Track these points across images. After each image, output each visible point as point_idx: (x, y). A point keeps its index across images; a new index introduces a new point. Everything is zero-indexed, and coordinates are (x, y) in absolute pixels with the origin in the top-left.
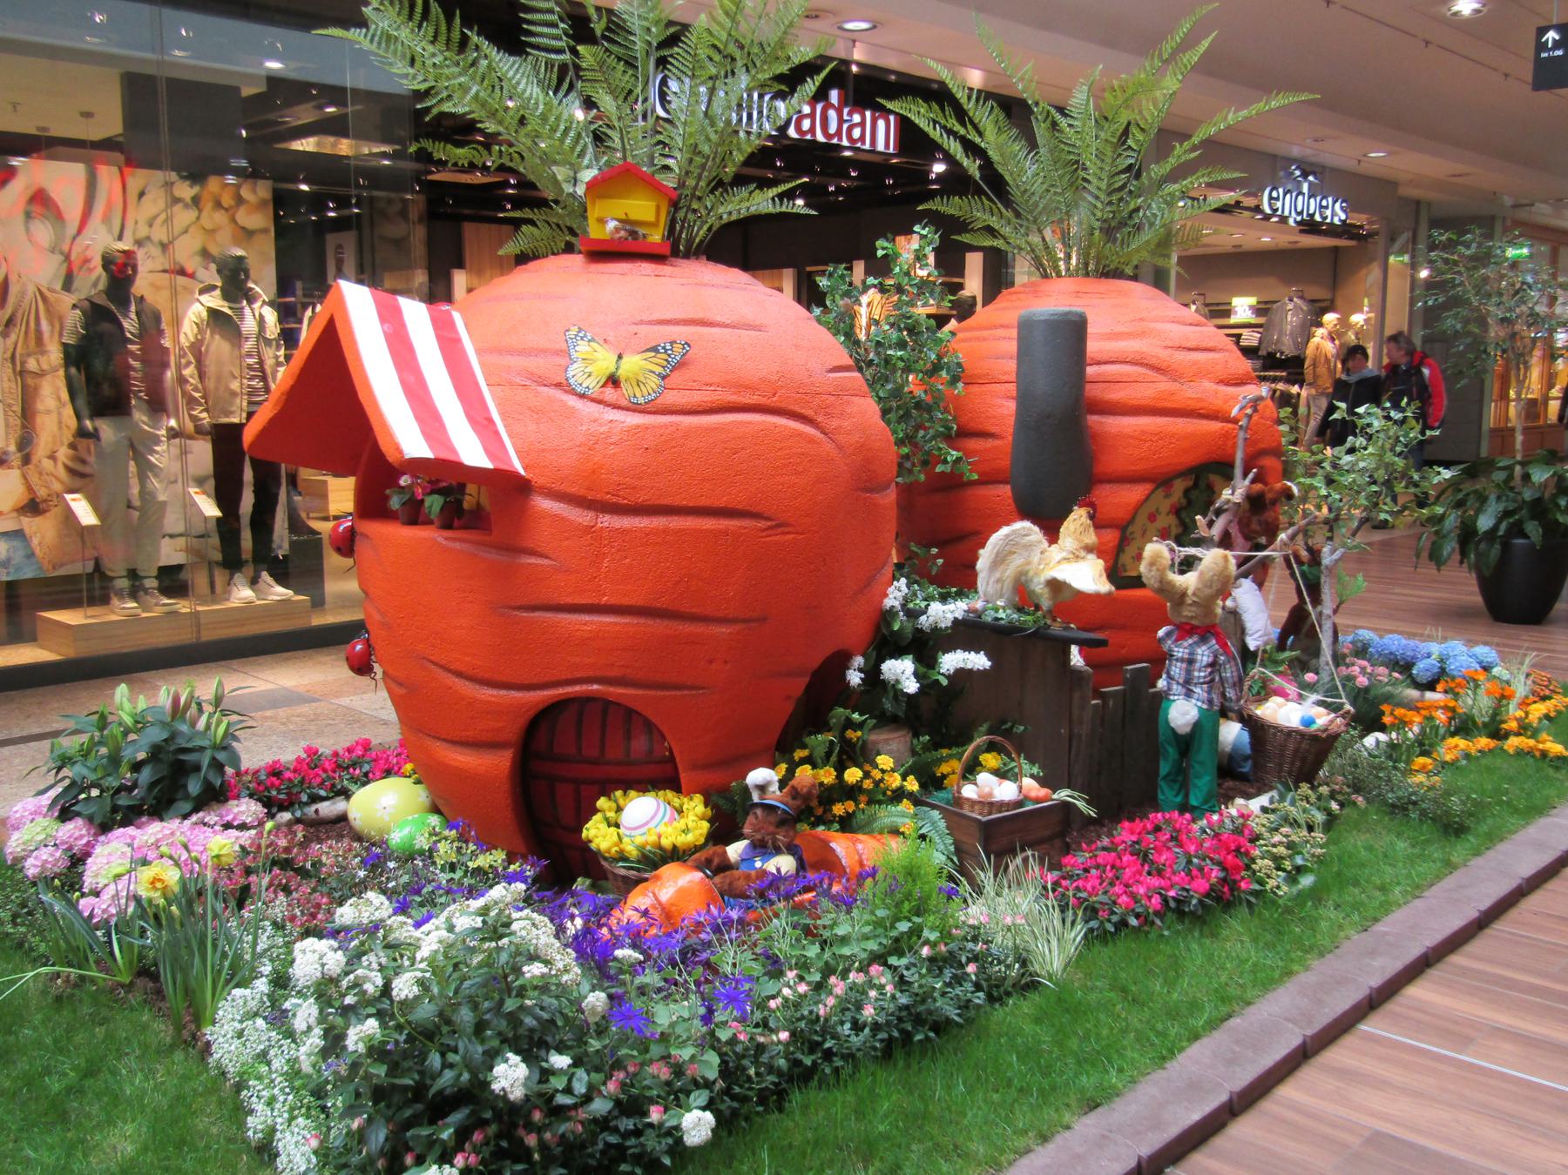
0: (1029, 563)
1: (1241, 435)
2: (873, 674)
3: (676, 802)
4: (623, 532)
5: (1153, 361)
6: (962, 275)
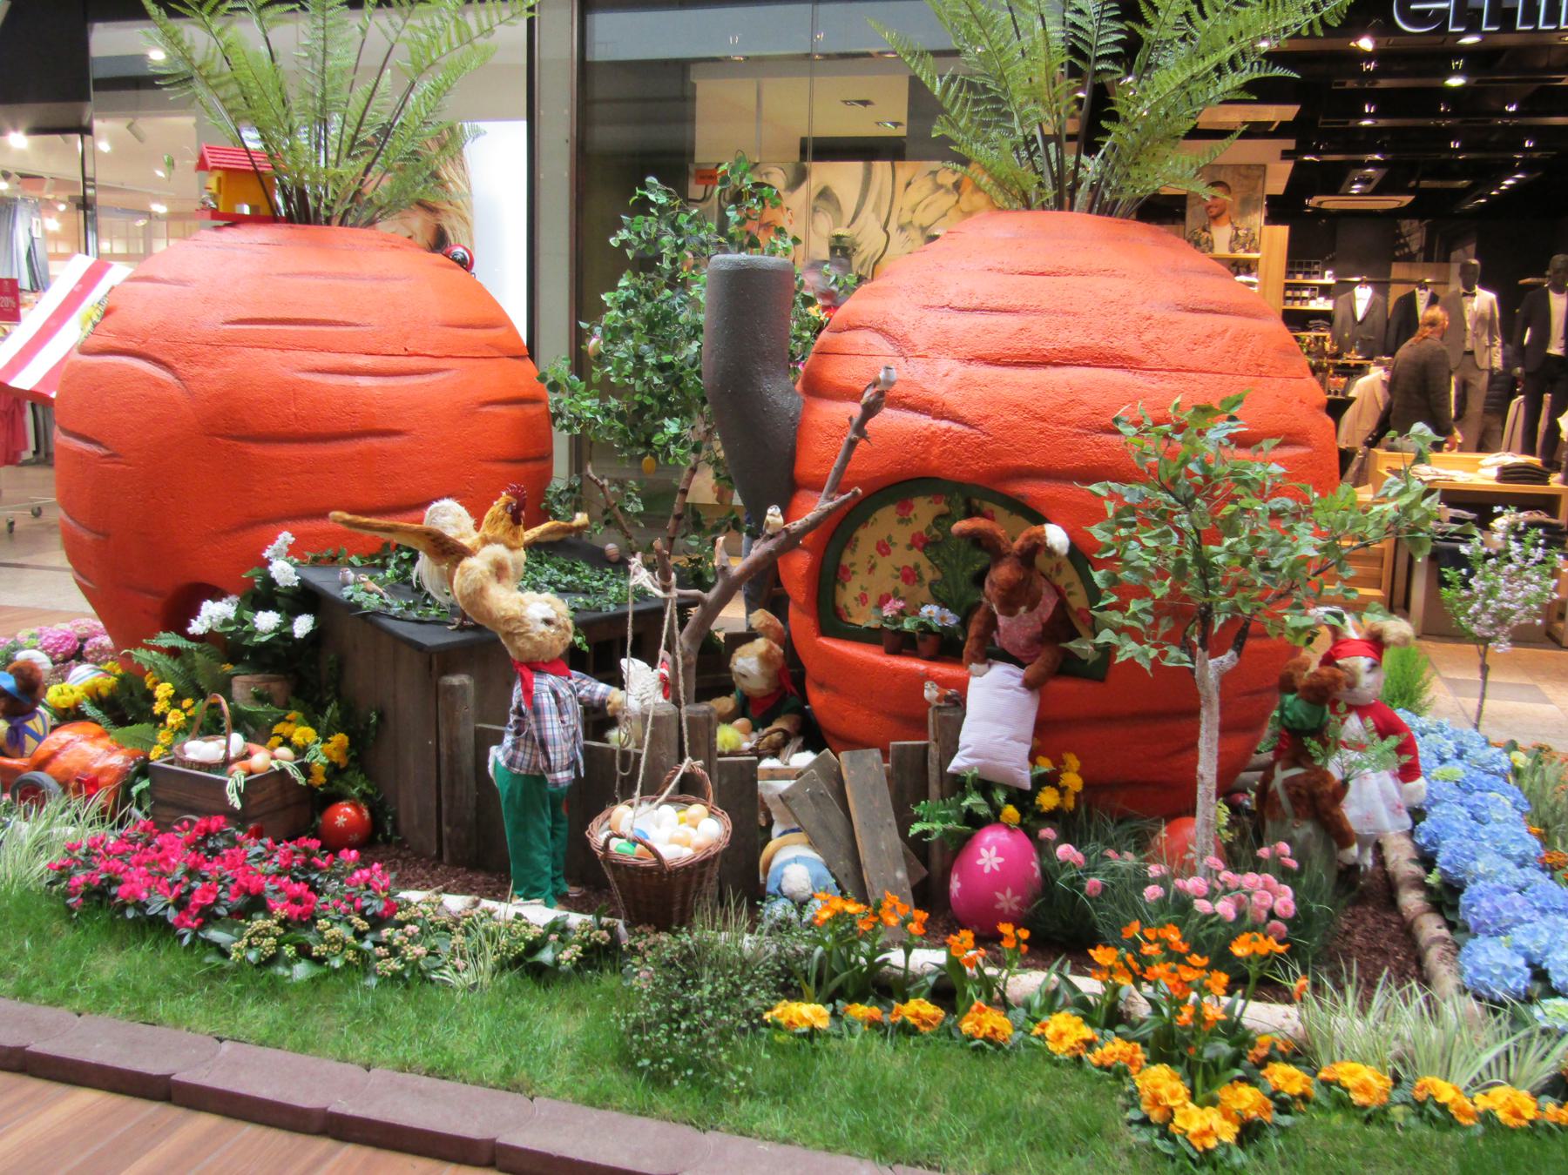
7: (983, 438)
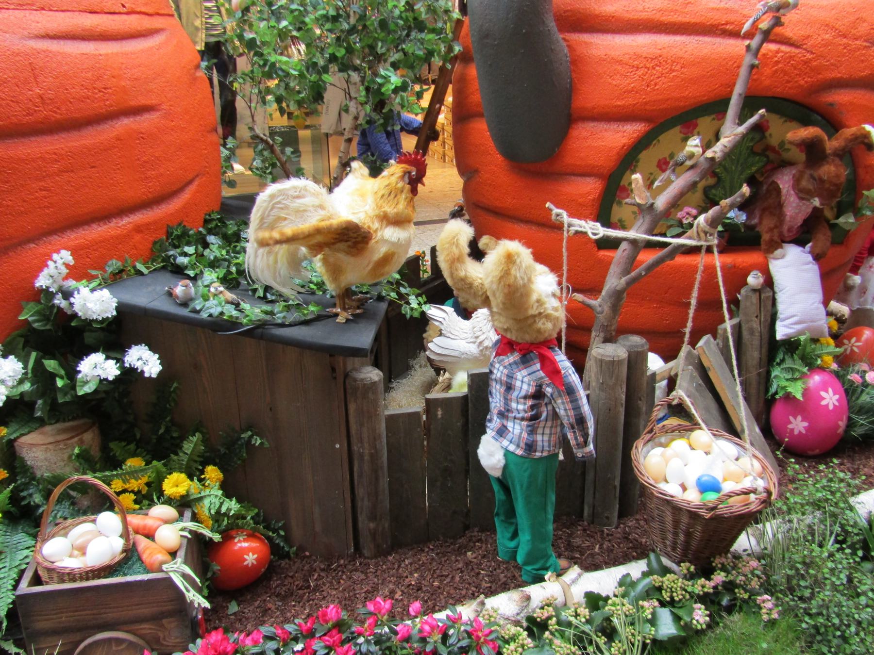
1: (748, 60)
7: (809, 56)
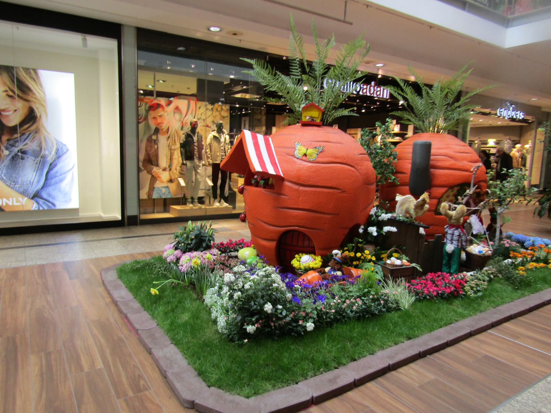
0: (410, 206)
1: (473, 176)
2: (365, 230)
3: (314, 257)
4: (305, 191)
5: (450, 155)
6: (407, 131)
